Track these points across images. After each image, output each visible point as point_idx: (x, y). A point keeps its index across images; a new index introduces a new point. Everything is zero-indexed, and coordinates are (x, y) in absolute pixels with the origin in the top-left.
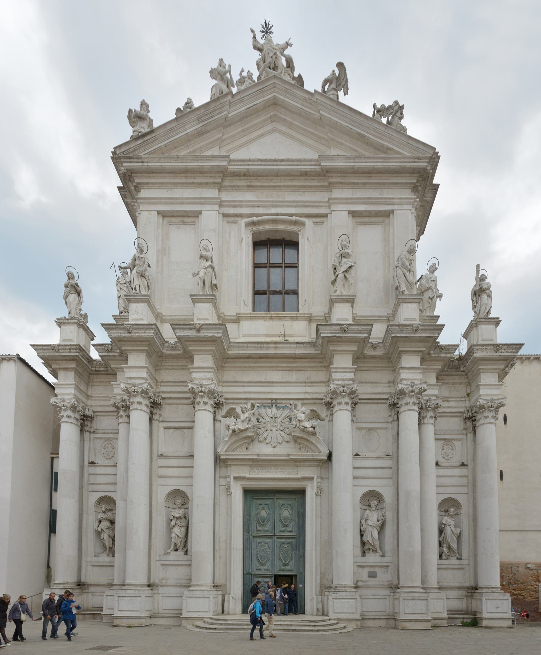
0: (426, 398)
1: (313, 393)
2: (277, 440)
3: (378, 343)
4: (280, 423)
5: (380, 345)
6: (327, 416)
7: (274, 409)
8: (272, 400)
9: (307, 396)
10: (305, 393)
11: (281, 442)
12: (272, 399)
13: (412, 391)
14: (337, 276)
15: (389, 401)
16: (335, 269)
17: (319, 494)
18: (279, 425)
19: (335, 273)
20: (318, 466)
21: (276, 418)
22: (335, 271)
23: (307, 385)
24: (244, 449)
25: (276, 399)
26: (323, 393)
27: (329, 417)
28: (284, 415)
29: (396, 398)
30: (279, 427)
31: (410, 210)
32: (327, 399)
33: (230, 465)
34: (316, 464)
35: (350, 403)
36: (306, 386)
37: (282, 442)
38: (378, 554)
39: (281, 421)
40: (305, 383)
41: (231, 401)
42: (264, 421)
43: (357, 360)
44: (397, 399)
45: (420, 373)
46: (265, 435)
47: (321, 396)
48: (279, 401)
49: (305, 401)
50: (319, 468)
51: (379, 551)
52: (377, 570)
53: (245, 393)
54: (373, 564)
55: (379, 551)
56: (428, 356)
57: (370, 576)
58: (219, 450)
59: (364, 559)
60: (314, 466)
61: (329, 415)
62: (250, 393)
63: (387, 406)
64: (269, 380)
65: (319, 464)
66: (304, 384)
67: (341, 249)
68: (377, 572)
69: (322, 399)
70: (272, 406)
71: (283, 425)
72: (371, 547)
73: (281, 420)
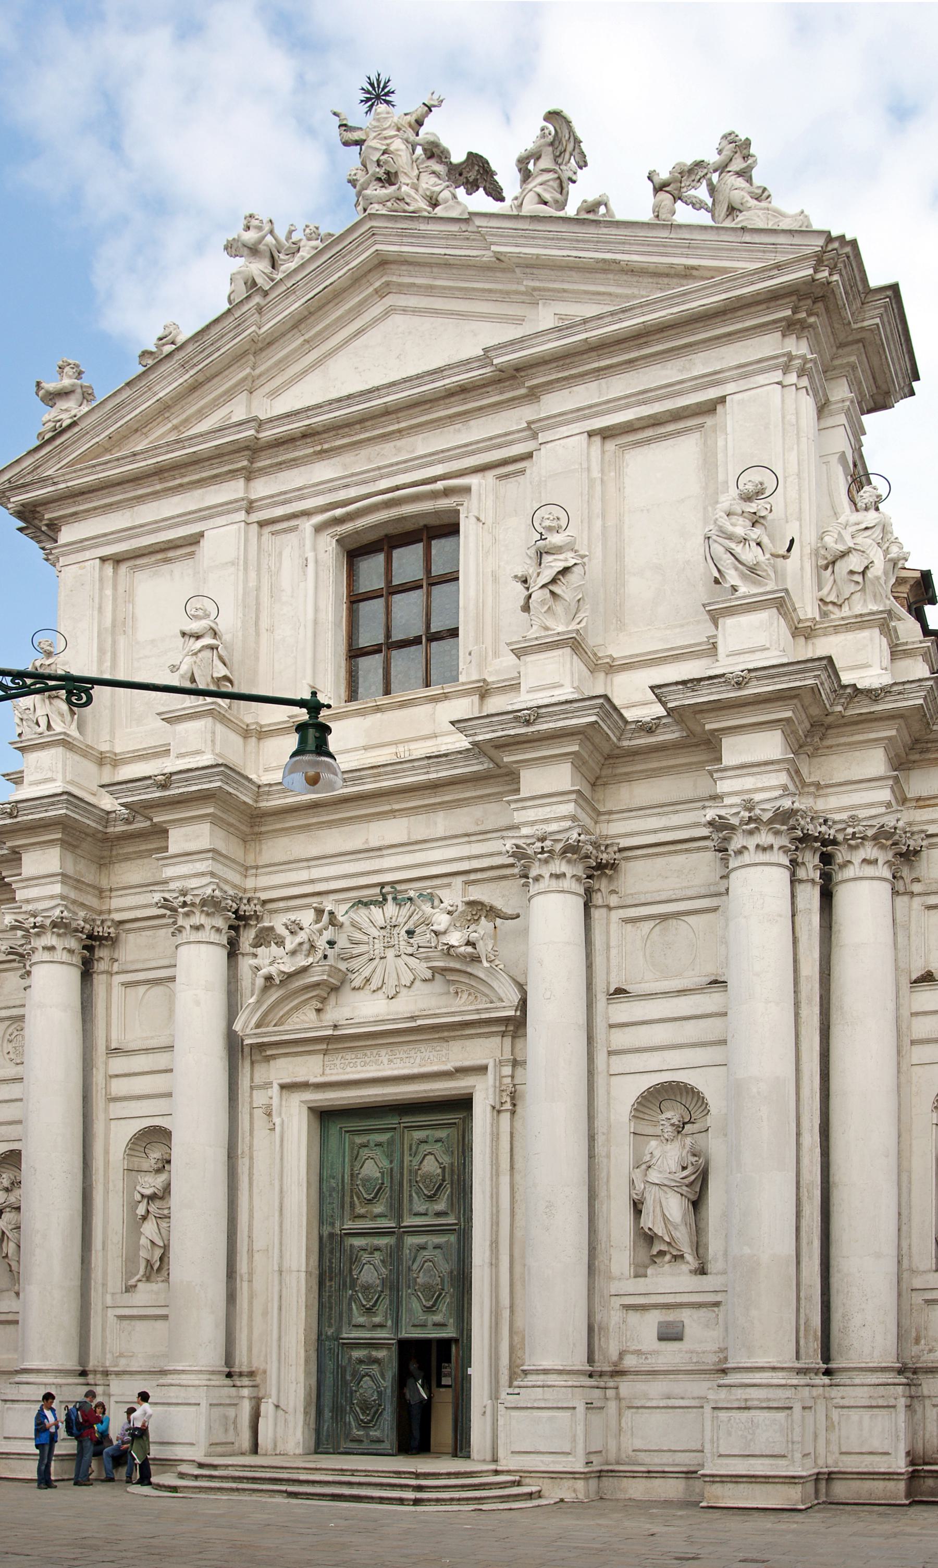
7: (390, 907)
8: (383, 888)
12: (382, 885)
17: (508, 1106)
20: (503, 1034)
21: (395, 926)
24: (312, 1015)
38: (685, 1268)
41: (281, 904)
42: (365, 938)
46: (366, 973)
51: (689, 1257)
52: (686, 1316)
54: (670, 1299)
55: (689, 1257)
57: (661, 1338)
58: (238, 1026)
59: (641, 1285)
65: (504, 1029)
68: (686, 1322)
70: (385, 900)
72: (664, 1248)
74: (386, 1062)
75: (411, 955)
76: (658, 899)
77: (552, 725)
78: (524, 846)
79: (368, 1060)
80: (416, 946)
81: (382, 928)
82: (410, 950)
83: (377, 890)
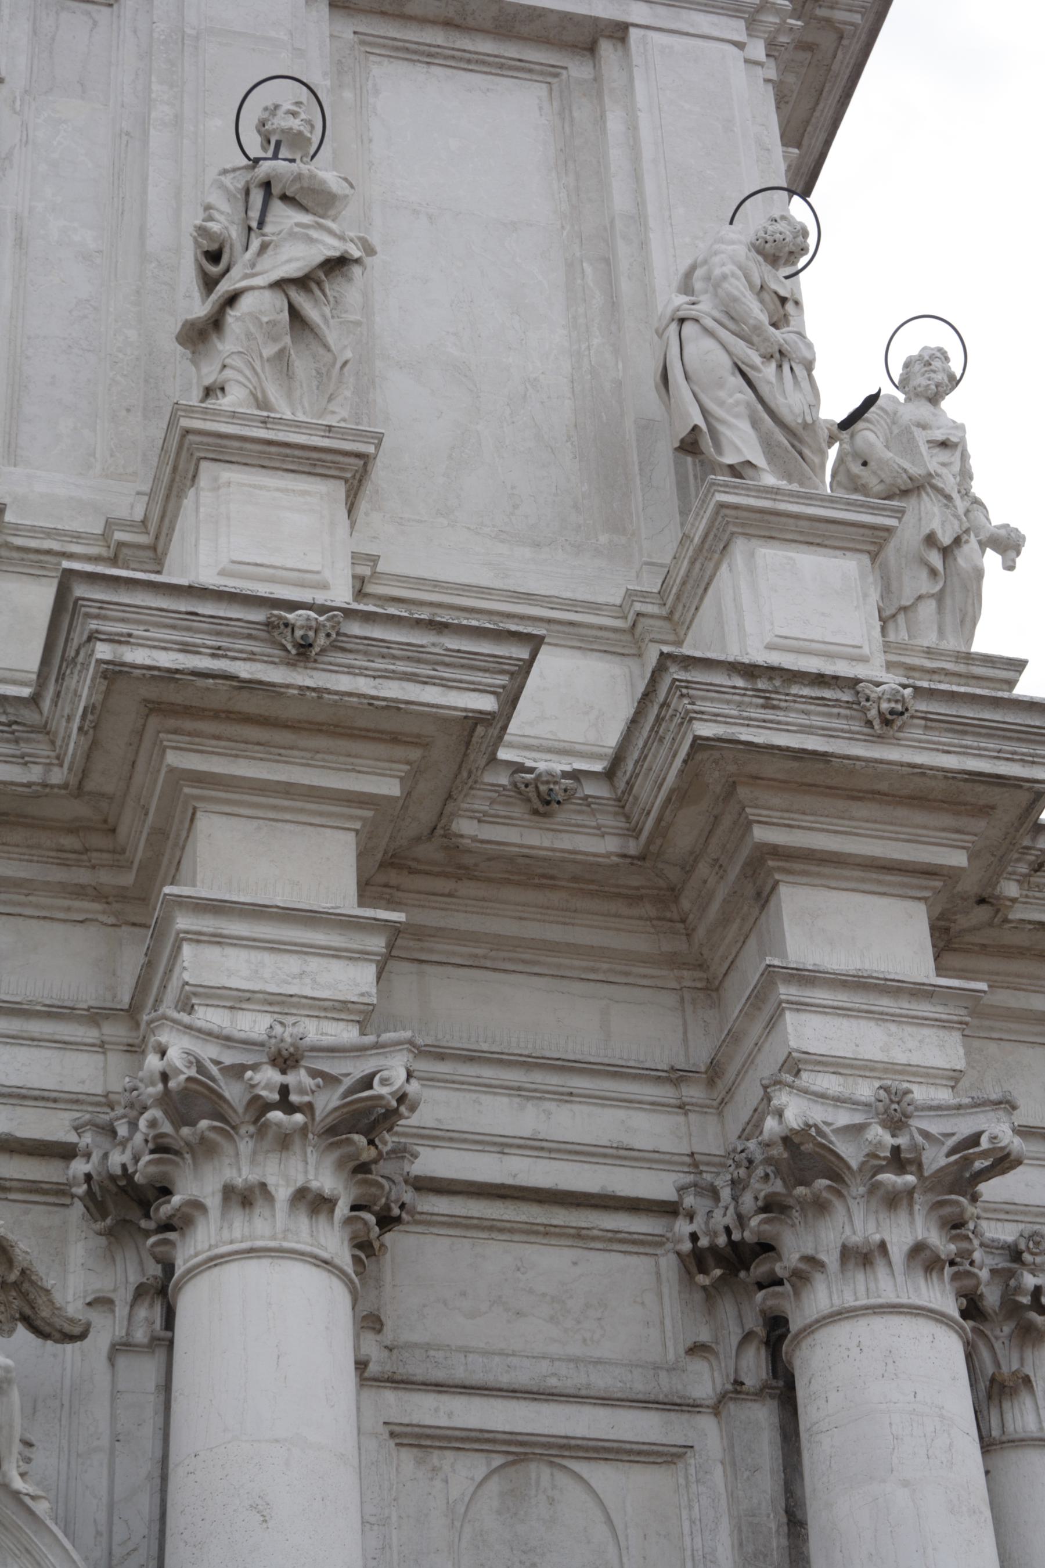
0: (1006, 1233)
3: (575, 775)
5: (590, 789)
13: (898, 1160)
14: (232, 299)
15: (683, 1227)
16: (214, 256)
19: (209, 283)
22: (214, 270)
26: (75, 1100)
27: (122, 1310)
29: (748, 1202)
31: (740, 45)
32: (117, 1159)
35: (342, 1209)
43: (393, 877)
44: (766, 1209)
45: (943, 1024)
56: (982, 913)
63: (669, 1264)
67: (254, 146)
76: (505, 1379)
77: (364, 685)
78: (214, 1070)
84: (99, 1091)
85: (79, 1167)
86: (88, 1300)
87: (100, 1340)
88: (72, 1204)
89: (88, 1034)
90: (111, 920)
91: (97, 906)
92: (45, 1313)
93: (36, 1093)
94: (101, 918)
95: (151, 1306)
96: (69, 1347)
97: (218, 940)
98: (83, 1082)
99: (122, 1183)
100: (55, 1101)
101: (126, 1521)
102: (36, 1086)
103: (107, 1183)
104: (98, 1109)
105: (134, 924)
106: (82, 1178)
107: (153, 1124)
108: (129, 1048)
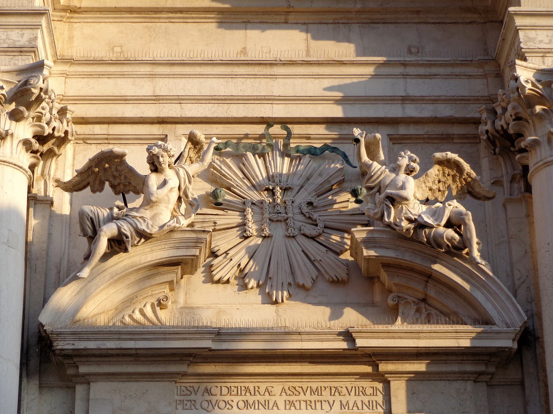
1: (435, 100)
2: (293, 273)
4: (305, 209)
6: (497, 183)
9: (411, 111)
10: (405, 99)
11: (308, 284)
12: (268, 122)
18: (301, 218)
20: (476, 378)
23: (411, 70)
25: (284, 122)
26: (477, 100)
27: (506, 185)
28: (320, 180)
30: (298, 221)
33: (87, 380)
34: (469, 368)
36: (405, 76)
37: (314, 281)
39: (310, 204)
40: (404, 64)
47: (471, 111)
48: (296, 129)
49: (403, 130)
50: (483, 388)
53: (157, 99)
60: (462, 376)
61: (506, 181)
62: (180, 100)
64: (252, 55)
65: (482, 368)
66: (399, 70)
69: (477, 122)
71: (315, 216)
73: (310, 199)
74: (281, 405)
75: (313, 238)
79: (251, 399)
80: (321, 225)
81: (267, 189)
82: (310, 230)
83: (260, 129)
84: (486, 94)
85: (482, 128)
86: (492, 182)
87: (501, 198)
88: (480, 142)
89: (480, 71)
90: (482, 21)
91: (476, 16)
92: (477, 190)
93: (460, 98)
94: (478, 20)
95: (519, 182)
96: (486, 202)
97: (534, 28)
98: (479, 92)
99: (502, 133)
100: (469, 100)
101: (519, 270)
102: (460, 95)
103: (495, 133)
104: (488, 102)
105: (492, 22)
106: (484, 132)
107: (514, 108)
108: (497, 75)
